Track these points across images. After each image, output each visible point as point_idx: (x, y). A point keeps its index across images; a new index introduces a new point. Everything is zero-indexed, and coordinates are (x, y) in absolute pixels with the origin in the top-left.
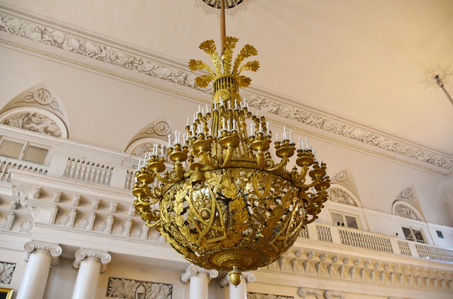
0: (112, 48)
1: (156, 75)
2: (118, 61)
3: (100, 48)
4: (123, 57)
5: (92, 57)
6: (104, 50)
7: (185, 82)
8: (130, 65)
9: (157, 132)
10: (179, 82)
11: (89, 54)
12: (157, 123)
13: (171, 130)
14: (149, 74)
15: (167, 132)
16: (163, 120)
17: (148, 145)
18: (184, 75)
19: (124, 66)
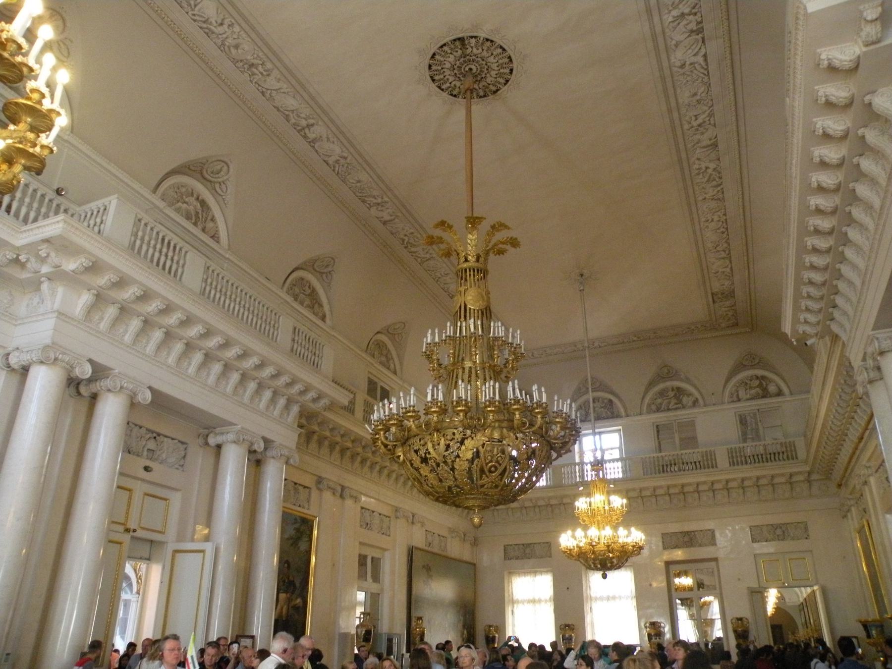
0: (242, 32)
1: (271, 98)
2: (233, 51)
3: (223, 20)
4: (247, 50)
5: (195, 21)
6: (225, 27)
7: (303, 129)
8: (246, 66)
9: (205, 172)
10: (295, 125)
11: (194, 15)
12: (214, 159)
13: (227, 179)
14: (263, 93)
15: (220, 180)
16: (226, 160)
17: (184, 190)
18: (311, 121)
19: (235, 61)
